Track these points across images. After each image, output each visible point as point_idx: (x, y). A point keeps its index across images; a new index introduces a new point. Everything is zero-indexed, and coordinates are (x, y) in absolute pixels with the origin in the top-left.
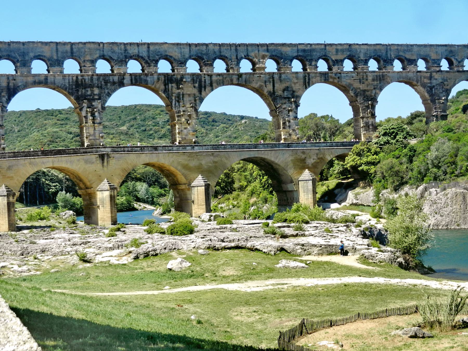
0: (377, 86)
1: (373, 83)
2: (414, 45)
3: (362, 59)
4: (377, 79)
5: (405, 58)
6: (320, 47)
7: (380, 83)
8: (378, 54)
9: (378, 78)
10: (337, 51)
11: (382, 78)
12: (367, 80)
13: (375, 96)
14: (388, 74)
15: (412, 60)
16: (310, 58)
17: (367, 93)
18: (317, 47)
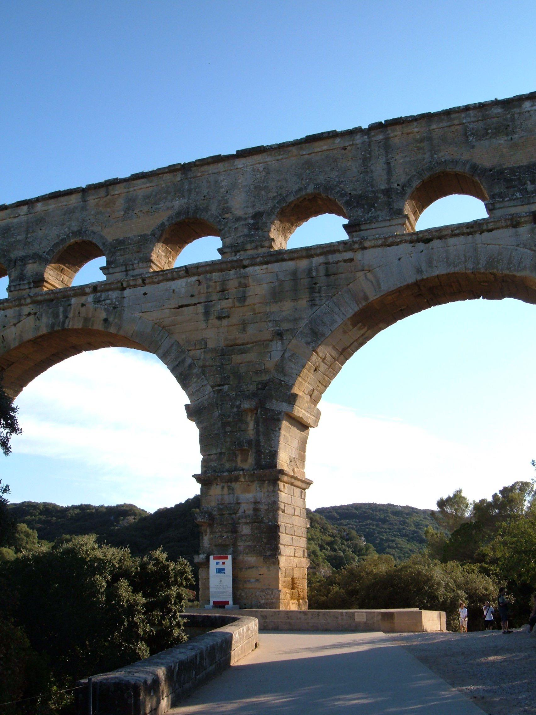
0: (296, 320)
1: (274, 308)
2: (519, 100)
3: (239, 213)
4: (295, 290)
5: (474, 168)
6: (63, 201)
7: (312, 303)
8: (321, 178)
9: (305, 281)
10: (131, 202)
11: (322, 281)
12: (243, 299)
13: (280, 367)
14: (358, 256)
15: (512, 170)
16: (22, 253)
17: (237, 358)
18: (52, 205)
